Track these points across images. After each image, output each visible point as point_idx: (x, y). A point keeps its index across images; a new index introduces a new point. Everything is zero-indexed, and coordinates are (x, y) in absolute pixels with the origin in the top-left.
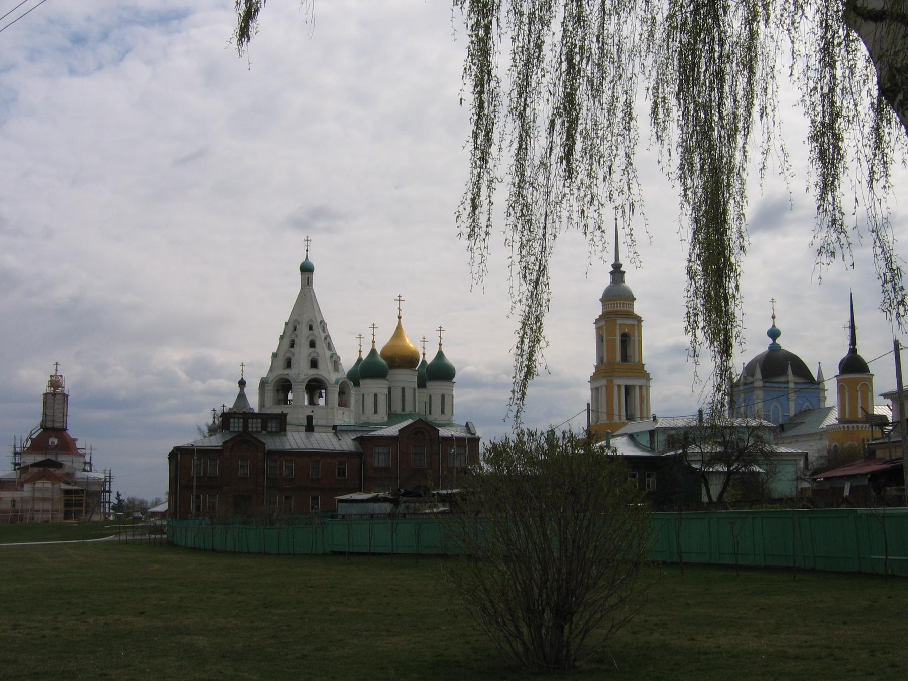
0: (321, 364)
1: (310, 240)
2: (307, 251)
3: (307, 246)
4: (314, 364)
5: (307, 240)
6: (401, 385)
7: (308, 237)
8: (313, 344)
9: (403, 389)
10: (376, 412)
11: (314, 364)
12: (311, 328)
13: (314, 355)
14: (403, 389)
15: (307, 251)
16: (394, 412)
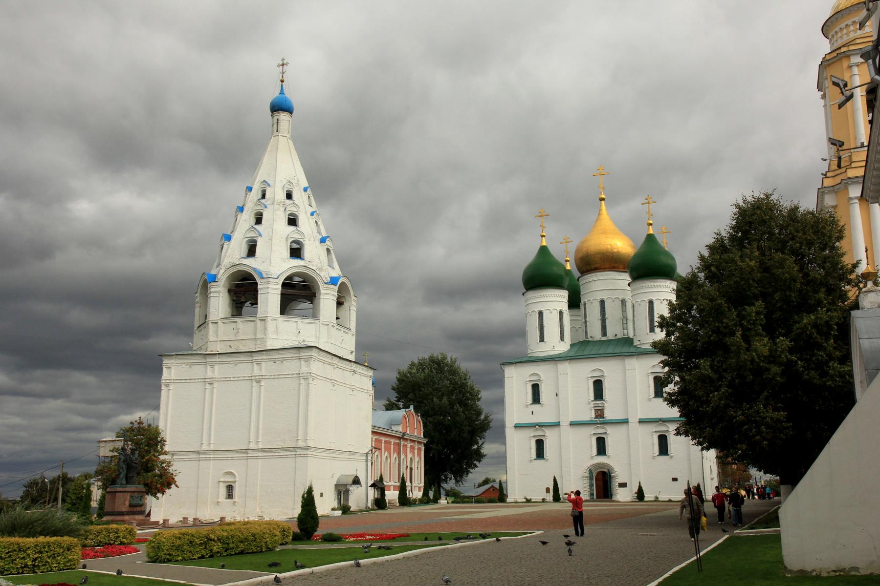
0: (307, 252)
1: (287, 64)
2: (282, 81)
3: (283, 73)
4: (252, 251)
5: (283, 65)
6: (600, 296)
7: (283, 60)
8: (259, 220)
9: (602, 302)
10: (542, 339)
11: (252, 251)
12: (264, 196)
13: (252, 234)
14: (602, 302)
15: (282, 81)
16: (591, 339)
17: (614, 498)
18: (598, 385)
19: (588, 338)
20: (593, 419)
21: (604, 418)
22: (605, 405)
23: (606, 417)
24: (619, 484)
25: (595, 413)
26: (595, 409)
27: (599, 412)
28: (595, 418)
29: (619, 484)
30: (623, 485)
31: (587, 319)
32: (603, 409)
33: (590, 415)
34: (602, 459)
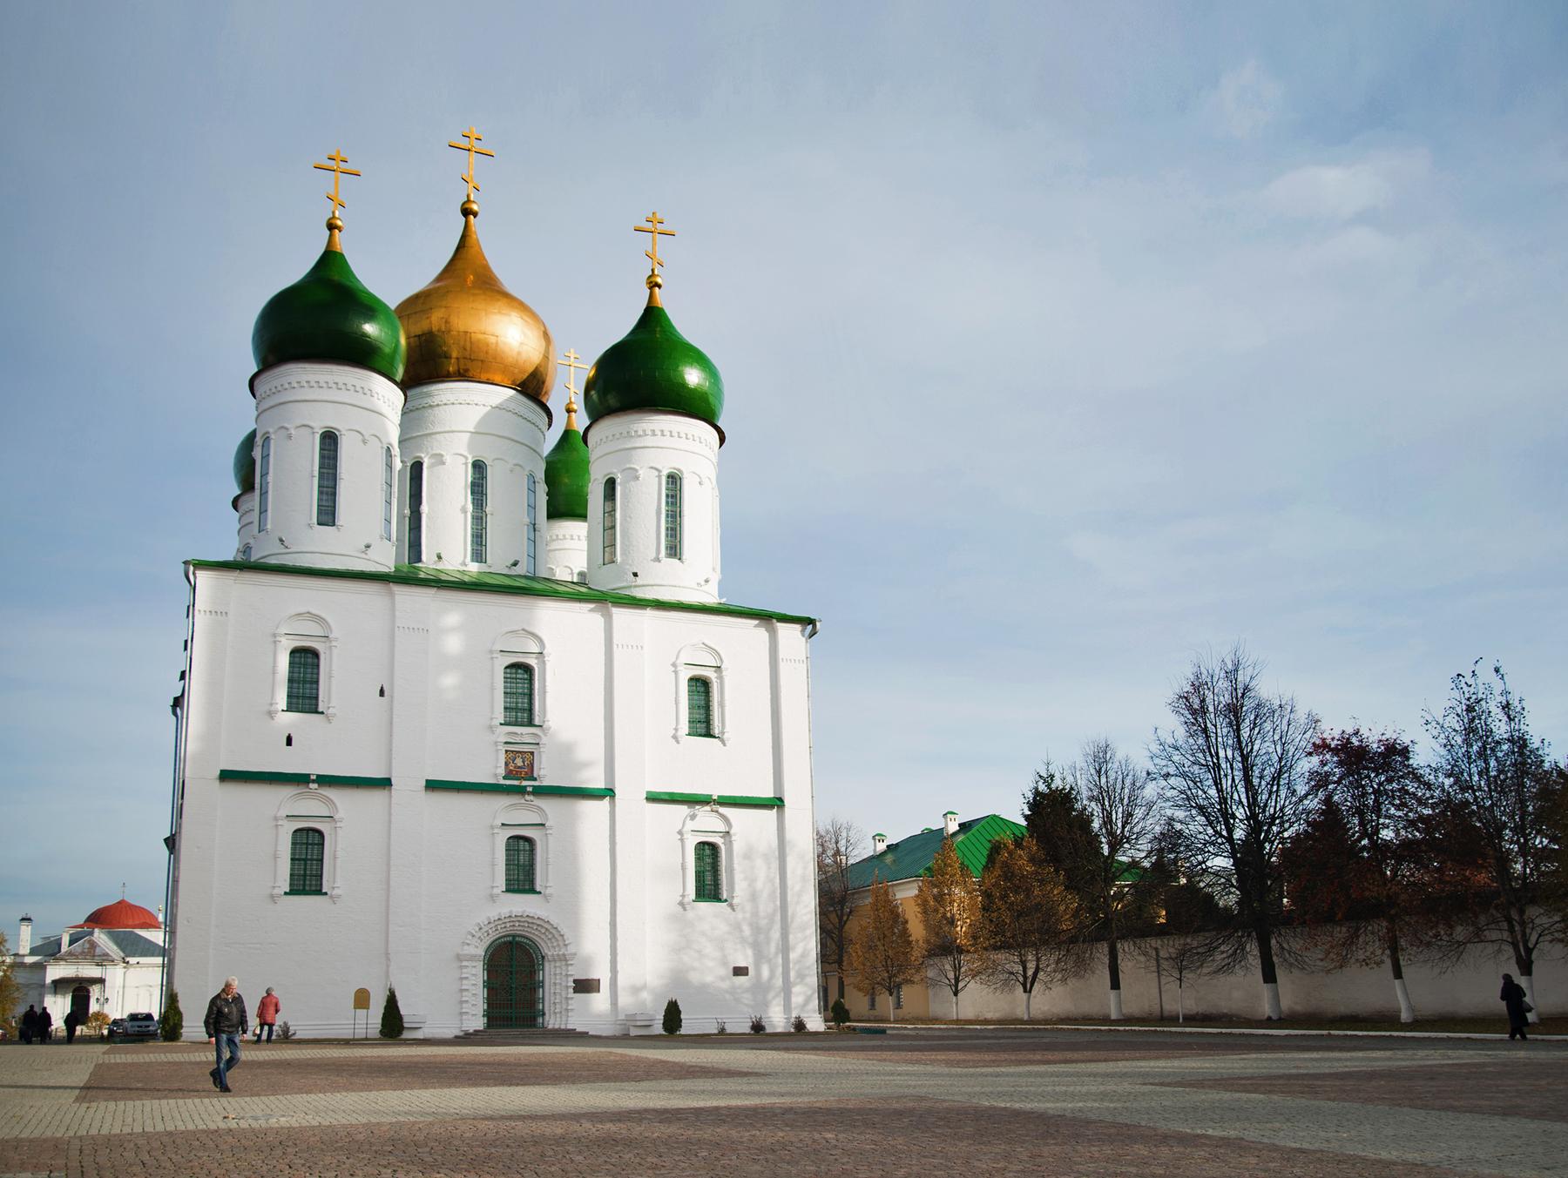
17: (552, 1022)
18: (521, 676)
19: (419, 560)
20: (503, 782)
21: (535, 779)
22: (544, 740)
23: (545, 776)
24: (575, 981)
25: (507, 764)
26: (506, 751)
27: (519, 762)
28: (504, 778)
29: (575, 981)
30: (585, 986)
31: (425, 508)
32: (532, 753)
33: (491, 769)
34: (522, 905)
